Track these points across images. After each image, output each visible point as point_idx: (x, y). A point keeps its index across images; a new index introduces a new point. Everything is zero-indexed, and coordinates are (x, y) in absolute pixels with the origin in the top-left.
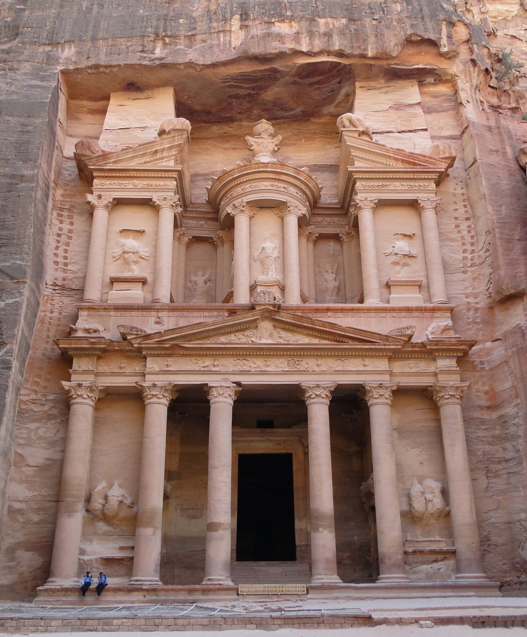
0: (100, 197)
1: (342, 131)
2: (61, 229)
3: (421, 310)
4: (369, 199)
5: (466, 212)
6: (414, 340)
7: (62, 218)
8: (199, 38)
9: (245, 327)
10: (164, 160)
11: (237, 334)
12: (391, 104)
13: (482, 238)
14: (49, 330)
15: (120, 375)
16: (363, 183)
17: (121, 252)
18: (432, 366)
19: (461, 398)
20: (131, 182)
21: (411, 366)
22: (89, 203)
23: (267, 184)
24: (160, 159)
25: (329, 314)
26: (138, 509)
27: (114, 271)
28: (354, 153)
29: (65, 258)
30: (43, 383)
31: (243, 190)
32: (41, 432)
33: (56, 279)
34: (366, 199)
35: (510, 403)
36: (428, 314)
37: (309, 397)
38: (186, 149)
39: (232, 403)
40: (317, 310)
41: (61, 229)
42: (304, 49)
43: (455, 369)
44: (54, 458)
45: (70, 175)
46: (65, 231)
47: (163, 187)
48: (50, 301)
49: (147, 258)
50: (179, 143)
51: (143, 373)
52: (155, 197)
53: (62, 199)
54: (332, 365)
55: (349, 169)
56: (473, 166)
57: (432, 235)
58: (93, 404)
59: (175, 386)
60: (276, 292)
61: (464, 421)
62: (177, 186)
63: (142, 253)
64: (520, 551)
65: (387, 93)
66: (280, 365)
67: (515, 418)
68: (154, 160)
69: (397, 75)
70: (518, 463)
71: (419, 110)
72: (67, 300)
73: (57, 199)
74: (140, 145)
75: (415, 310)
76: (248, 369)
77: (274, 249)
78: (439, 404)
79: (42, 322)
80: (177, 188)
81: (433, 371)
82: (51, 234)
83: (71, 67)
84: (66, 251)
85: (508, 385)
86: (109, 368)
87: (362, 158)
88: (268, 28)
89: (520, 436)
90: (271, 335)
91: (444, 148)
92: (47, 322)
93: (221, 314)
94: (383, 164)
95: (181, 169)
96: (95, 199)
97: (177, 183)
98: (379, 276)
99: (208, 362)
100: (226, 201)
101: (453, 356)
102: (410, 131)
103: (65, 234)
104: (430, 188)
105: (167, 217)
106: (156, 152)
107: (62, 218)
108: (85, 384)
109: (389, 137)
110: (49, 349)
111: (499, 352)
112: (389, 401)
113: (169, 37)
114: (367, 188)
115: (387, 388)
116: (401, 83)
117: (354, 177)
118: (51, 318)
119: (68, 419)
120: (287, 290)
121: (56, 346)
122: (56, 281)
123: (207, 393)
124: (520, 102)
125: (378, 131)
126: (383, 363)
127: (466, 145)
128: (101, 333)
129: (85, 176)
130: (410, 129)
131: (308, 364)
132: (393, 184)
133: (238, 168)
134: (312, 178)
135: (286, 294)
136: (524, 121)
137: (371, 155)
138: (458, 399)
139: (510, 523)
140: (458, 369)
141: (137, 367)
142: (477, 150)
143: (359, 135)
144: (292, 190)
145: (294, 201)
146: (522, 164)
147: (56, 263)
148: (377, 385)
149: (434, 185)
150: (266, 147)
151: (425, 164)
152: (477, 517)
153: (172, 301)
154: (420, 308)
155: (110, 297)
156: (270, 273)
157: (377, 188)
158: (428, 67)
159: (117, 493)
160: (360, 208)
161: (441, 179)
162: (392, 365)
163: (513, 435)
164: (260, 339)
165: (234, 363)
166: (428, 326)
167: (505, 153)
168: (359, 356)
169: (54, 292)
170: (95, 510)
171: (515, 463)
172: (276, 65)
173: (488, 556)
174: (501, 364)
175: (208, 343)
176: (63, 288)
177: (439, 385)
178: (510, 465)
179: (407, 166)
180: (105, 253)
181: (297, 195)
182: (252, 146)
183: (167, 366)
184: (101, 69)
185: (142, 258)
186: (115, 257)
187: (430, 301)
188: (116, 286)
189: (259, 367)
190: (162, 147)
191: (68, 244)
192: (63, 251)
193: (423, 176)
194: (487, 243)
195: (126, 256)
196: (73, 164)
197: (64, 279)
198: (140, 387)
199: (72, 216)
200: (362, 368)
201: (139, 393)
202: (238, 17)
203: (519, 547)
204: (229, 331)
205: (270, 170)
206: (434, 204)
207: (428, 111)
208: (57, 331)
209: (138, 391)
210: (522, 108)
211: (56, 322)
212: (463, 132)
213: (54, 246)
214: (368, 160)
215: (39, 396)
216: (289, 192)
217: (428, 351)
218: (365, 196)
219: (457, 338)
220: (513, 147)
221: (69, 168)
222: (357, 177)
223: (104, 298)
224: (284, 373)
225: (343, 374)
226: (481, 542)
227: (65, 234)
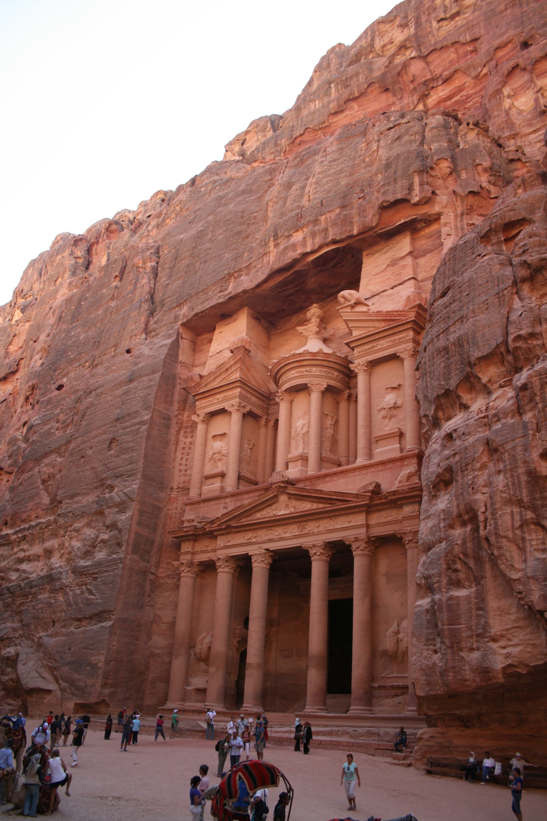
0: (198, 416)
2: (185, 443)
3: (393, 461)
4: (361, 363)
8: (253, 265)
12: (388, 262)
21: (385, 515)
23: (293, 372)
24: (232, 373)
25: (328, 479)
29: (186, 465)
33: (179, 483)
36: (398, 464)
42: (308, 250)
63: (224, 452)
65: (386, 252)
66: (294, 531)
69: (391, 235)
71: (409, 261)
77: (304, 425)
79: (171, 518)
83: (185, 320)
84: (187, 460)
87: (356, 327)
88: (288, 241)
90: (287, 506)
91: (414, 297)
94: (371, 327)
99: (250, 535)
102: (400, 284)
106: (227, 369)
113: (236, 272)
114: (361, 353)
116: (397, 238)
130: (400, 282)
144: (314, 369)
145: (316, 379)
149: (411, 334)
157: (368, 351)
158: (407, 220)
168: (345, 514)
172: (297, 268)
179: (388, 323)
182: (302, 333)
184: (200, 315)
191: (188, 454)
193: (400, 329)
195: (215, 456)
197: (184, 483)
200: (346, 525)
202: (272, 238)
214: (360, 327)
224: (296, 537)
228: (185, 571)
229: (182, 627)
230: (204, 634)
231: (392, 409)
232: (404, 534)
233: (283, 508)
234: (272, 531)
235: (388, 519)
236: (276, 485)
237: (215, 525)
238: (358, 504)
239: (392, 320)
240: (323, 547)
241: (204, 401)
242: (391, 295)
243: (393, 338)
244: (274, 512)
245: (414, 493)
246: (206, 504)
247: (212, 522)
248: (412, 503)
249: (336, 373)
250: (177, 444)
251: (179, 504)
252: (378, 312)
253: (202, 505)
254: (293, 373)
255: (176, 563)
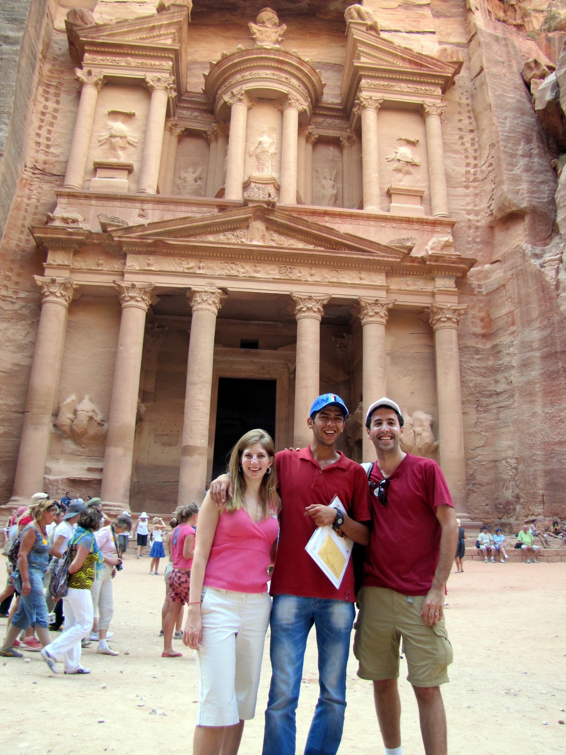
0: (90, 73)
1: (350, 23)
2: (45, 107)
3: (422, 222)
4: (373, 98)
5: (471, 123)
6: (414, 254)
7: (48, 96)
9: (235, 226)
10: (161, 38)
11: (226, 233)
13: (486, 152)
14: (25, 219)
15: (96, 274)
16: (369, 81)
17: (108, 136)
18: (430, 284)
19: (458, 322)
20: (125, 59)
21: (409, 283)
22: (78, 79)
24: (157, 36)
25: (327, 218)
26: (109, 427)
27: (99, 156)
28: (361, 48)
30: (14, 278)
31: (242, 77)
32: (9, 333)
34: (371, 98)
35: (506, 330)
37: (300, 310)
38: (185, 27)
39: (216, 311)
40: (314, 213)
41: (45, 107)
43: (453, 289)
44: (23, 364)
45: (60, 49)
46: (50, 110)
47: (158, 67)
48: (28, 186)
49: (135, 144)
50: (178, 20)
51: (122, 272)
52: (150, 77)
53: (49, 74)
54: (326, 276)
55: (355, 64)
56: (479, 76)
57: (436, 143)
58: (66, 304)
59: (156, 288)
60: (271, 189)
61: (459, 349)
62: (173, 68)
63: (130, 138)
64: (504, 490)
67: (509, 347)
68: (151, 37)
70: (509, 396)
72: (46, 187)
73: (44, 74)
74: (137, 19)
75: (416, 222)
76: (236, 274)
77: (271, 144)
78: (435, 327)
79: (18, 208)
80: (173, 70)
81: (430, 290)
82: (35, 111)
84: (49, 132)
85: (504, 311)
86: (85, 264)
87: (369, 54)
89: (513, 367)
90: (263, 237)
91: (452, 52)
92: (23, 209)
93: (211, 210)
95: (178, 48)
96: (84, 75)
97: (173, 65)
98: (380, 183)
99: (192, 264)
100: (223, 89)
101: (452, 276)
103: (49, 113)
104: (436, 93)
105: (160, 100)
106: (153, 28)
107: (48, 96)
108: (59, 280)
109: (397, 36)
110: (24, 241)
111: (498, 274)
112: (384, 321)
114: (372, 86)
115: (383, 306)
117: (360, 73)
118: (28, 205)
119: (38, 321)
120: (282, 189)
121: (31, 237)
122: (36, 164)
123: (190, 299)
124: (526, 19)
125: (386, 29)
126: (380, 277)
127: (473, 53)
128: (80, 224)
129: (76, 51)
131: (301, 273)
132: (398, 85)
133: (239, 53)
134: (315, 72)
135: (281, 194)
136: (529, 38)
137: (378, 52)
138: (454, 323)
139: (496, 461)
140: (456, 289)
141: (116, 266)
142: (484, 58)
143: (367, 30)
144: (294, 82)
146: (527, 80)
147: (38, 144)
148: (372, 302)
149: (439, 91)
150: (269, 37)
151: (432, 67)
152: (465, 453)
153: (158, 192)
154: (421, 220)
155: (92, 184)
156: (266, 170)
157: (382, 87)
159: (87, 406)
160: (364, 107)
161: (447, 85)
162: (389, 280)
163: (507, 366)
164: (251, 241)
165: (221, 266)
166: (428, 241)
167: (510, 66)
169: (33, 176)
170: (63, 425)
171: (506, 396)
173: (473, 496)
174: (498, 289)
175: (194, 242)
176: (43, 172)
177: (437, 306)
178: (501, 399)
179: (414, 67)
180: (91, 136)
181: (298, 88)
182: (255, 34)
183: (149, 265)
185: (129, 144)
186: (100, 141)
187: (431, 214)
188: (100, 172)
189: (248, 272)
190: (160, 23)
191: (52, 124)
192: (46, 132)
194: (490, 156)
195: (113, 140)
196: (65, 37)
197: (45, 163)
198: (117, 288)
199: (59, 94)
200: (357, 282)
201: (116, 296)
203: (504, 486)
204: (218, 229)
205: (272, 56)
206: (439, 111)
207: (437, 15)
208: (33, 220)
209: (115, 294)
210: (526, 27)
211: (33, 210)
212: (470, 40)
213: (37, 125)
214: (375, 57)
215: (10, 293)
216: (292, 83)
217: (427, 268)
218: (370, 94)
219: (457, 255)
220: (519, 63)
221: (59, 42)
222: (363, 73)
223: (86, 185)
225: (336, 286)
226: (467, 480)
227: (49, 113)
228: (58, 294)
229: (46, 379)
230: (73, 397)
231: (409, 165)
232: (440, 308)
233: (257, 236)
234: (233, 266)
235: (411, 288)
236: (256, 204)
237: (132, 235)
238: (386, 259)
239: (422, 66)
240: (325, 302)
241: (100, 58)
242: (408, 39)
243: (419, 87)
244: (244, 240)
245: (462, 266)
246: (105, 203)
247: (129, 229)
248: (449, 277)
249: (309, 100)
250: (34, 105)
251: (35, 192)
252: (406, 48)
253: (93, 202)
254: (267, 73)
255: (38, 279)
